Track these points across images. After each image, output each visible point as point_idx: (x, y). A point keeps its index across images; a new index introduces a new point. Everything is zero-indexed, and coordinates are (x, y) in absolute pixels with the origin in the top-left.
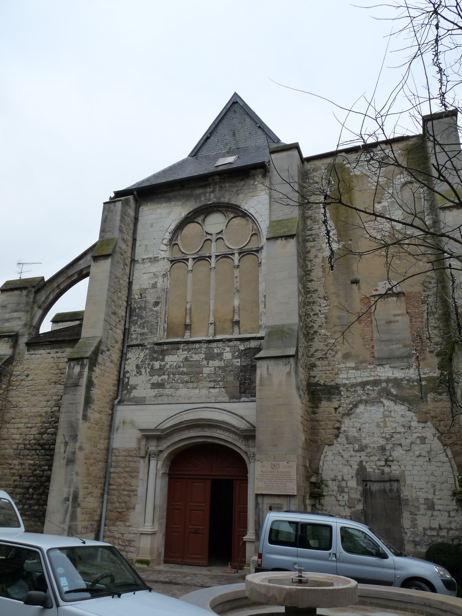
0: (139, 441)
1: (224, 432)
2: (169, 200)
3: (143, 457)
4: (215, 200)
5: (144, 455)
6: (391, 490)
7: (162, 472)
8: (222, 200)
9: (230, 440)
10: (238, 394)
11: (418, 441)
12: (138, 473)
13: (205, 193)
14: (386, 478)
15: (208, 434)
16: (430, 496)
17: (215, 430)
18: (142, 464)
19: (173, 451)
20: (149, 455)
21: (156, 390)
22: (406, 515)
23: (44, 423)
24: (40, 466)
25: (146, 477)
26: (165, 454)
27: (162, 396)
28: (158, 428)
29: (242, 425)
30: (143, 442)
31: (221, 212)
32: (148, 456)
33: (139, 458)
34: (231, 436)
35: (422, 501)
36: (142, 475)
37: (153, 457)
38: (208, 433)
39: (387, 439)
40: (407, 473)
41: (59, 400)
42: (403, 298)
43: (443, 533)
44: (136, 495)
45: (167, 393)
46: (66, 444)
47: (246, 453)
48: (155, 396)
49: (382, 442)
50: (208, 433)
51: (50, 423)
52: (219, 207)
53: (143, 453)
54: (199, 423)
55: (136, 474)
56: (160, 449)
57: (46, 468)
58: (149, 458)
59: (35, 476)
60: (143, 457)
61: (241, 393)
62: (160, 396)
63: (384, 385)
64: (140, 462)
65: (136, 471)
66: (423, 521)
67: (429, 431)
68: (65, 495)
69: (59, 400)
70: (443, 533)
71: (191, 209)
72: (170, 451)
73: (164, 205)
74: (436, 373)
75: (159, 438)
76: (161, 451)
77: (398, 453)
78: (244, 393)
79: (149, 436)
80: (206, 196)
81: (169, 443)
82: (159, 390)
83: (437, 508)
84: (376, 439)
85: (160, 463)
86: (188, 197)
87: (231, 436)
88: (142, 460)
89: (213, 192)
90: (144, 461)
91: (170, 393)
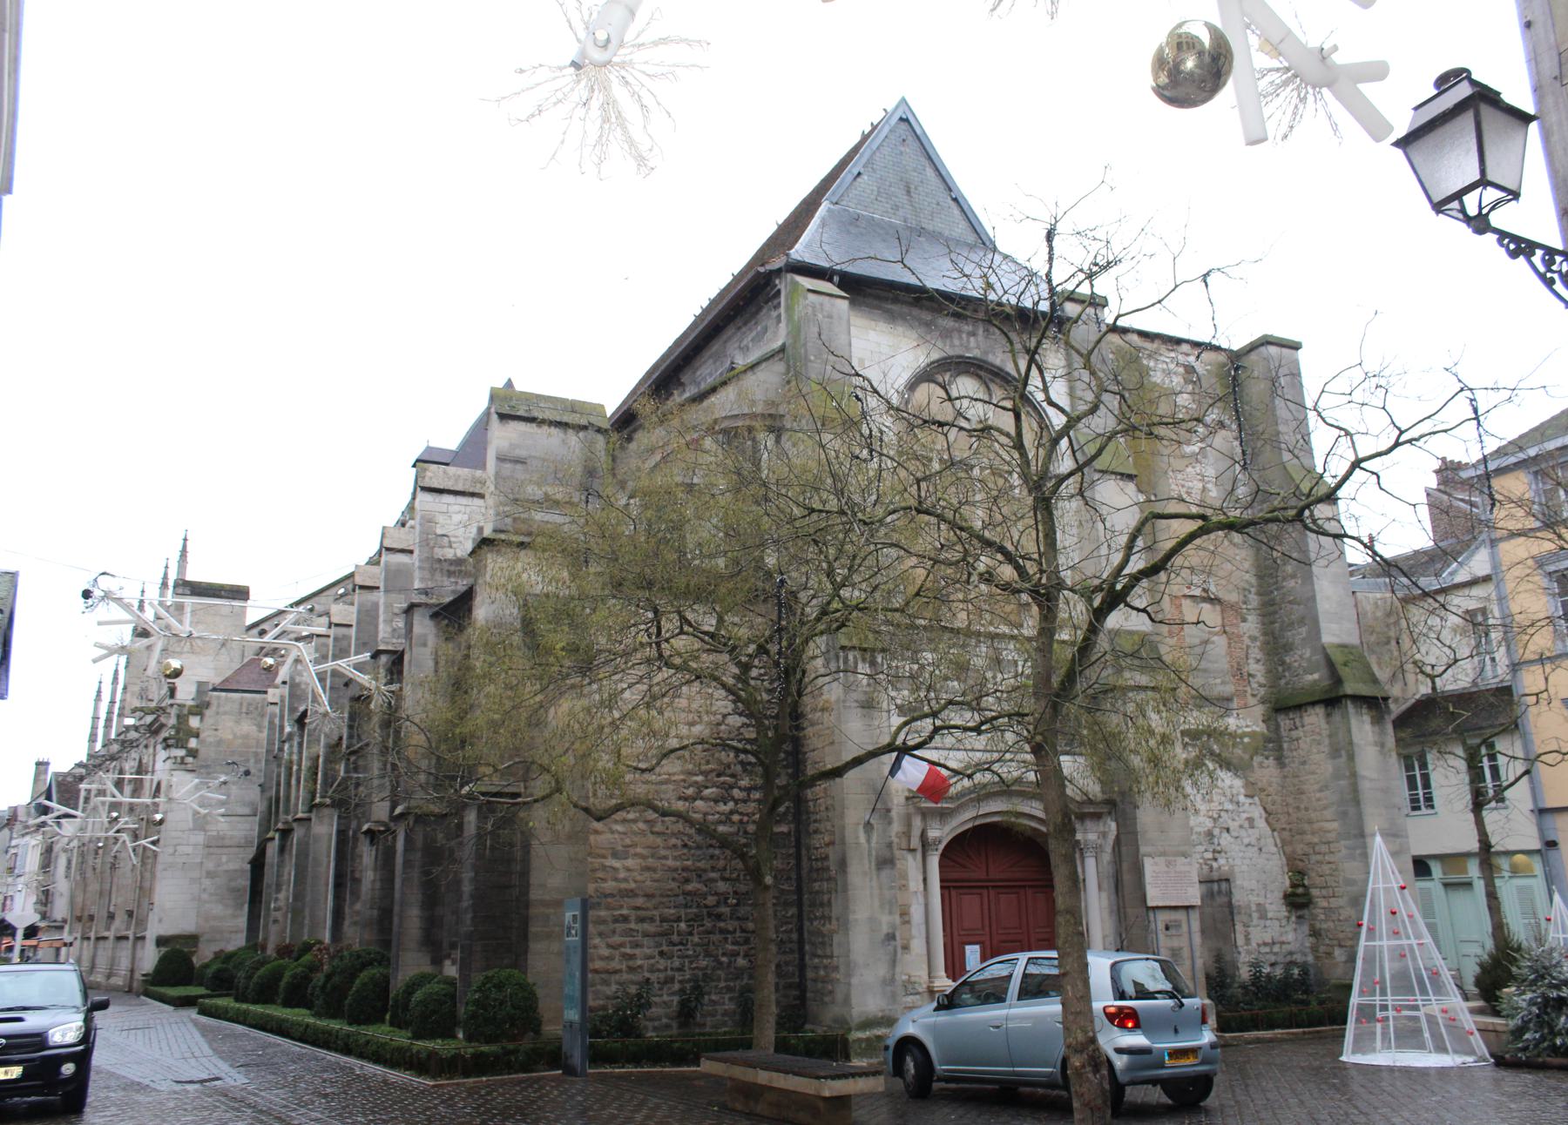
2: (892, 318)
4: (976, 353)
6: (1220, 892)
8: (990, 358)
11: (1246, 825)
13: (960, 331)
14: (1215, 876)
16: (1261, 900)
22: (1239, 927)
23: (690, 773)
24: (700, 874)
31: (980, 377)
35: (1254, 908)
39: (1215, 820)
40: (1237, 869)
41: (719, 724)
42: (1218, 608)
43: (1276, 949)
46: (868, 826)
49: (1209, 824)
51: (705, 773)
52: (980, 368)
57: (713, 875)
59: (686, 894)
63: (1205, 738)
66: (1258, 935)
67: (1257, 813)
68: (885, 929)
69: (719, 724)
70: (1276, 949)
71: (935, 356)
73: (883, 326)
74: (1260, 728)
77: (1225, 840)
80: (961, 338)
83: (1270, 915)
84: (1201, 819)
86: (946, 334)
88: (910, 857)
89: (974, 334)
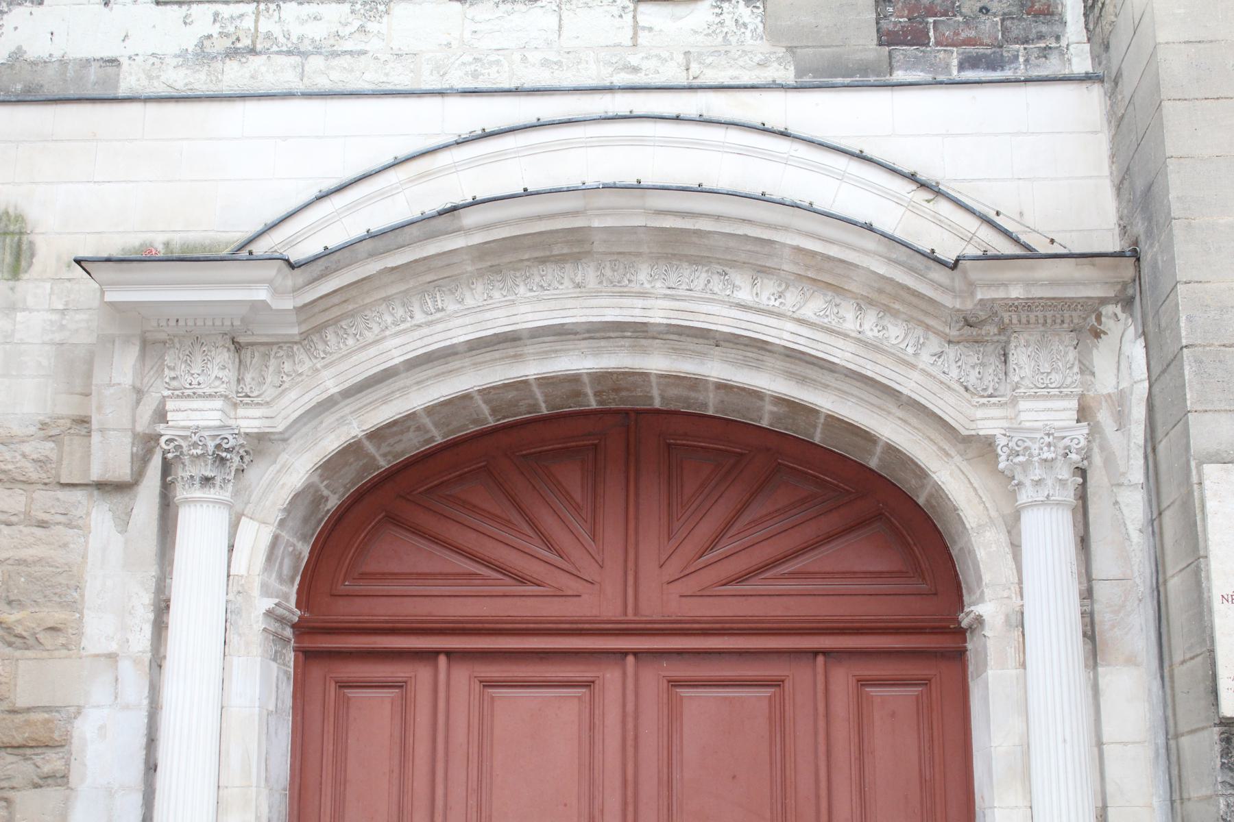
0: (79, 369)
1: (791, 298)
3: (106, 487)
5: (123, 472)
7: (270, 603)
9: (841, 353)
10: (865, 45)
12: (74, 606)
15: (658, 313)
17: (717, 285)
18: (107, 546)
19: (352, 450)
20: (167, 467)
21: (203, 13)
25: (142, 640)
26: (295, 470)
27: (253, 51)
28: (260, 248)
29: (944, 233)
30: (123, 368)
32: (162, 473)
33: (78, 495)
34: (850, 323)
36: (110, 614)
37: (207, 481)
38: (656, 299)
44: (60, 779)
45: (296, 31)
47: (981, 449)
48: (202, 55)
50: (656, 299)
53: (110, 455)
54: (596, 223)
55: (57, 616)
56: (250, 421)
58: (166, 489)
60: (106, 487)
61: (888, 38)
62: (232, 53)
64: (84, 529)
65: (63, 588)
72: (331, 442)
75: (242, 341)
76: (260, 445)
78: (918, 38)
79: (178, 305)
81: (331, 383)
82: (226, 10)
85: (255, 538)
87: (850, 323)
88: (100, 517)
90: (123, 521)
91: (317, 31)
